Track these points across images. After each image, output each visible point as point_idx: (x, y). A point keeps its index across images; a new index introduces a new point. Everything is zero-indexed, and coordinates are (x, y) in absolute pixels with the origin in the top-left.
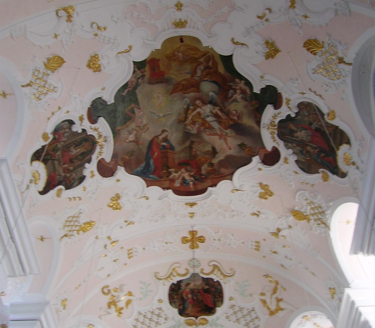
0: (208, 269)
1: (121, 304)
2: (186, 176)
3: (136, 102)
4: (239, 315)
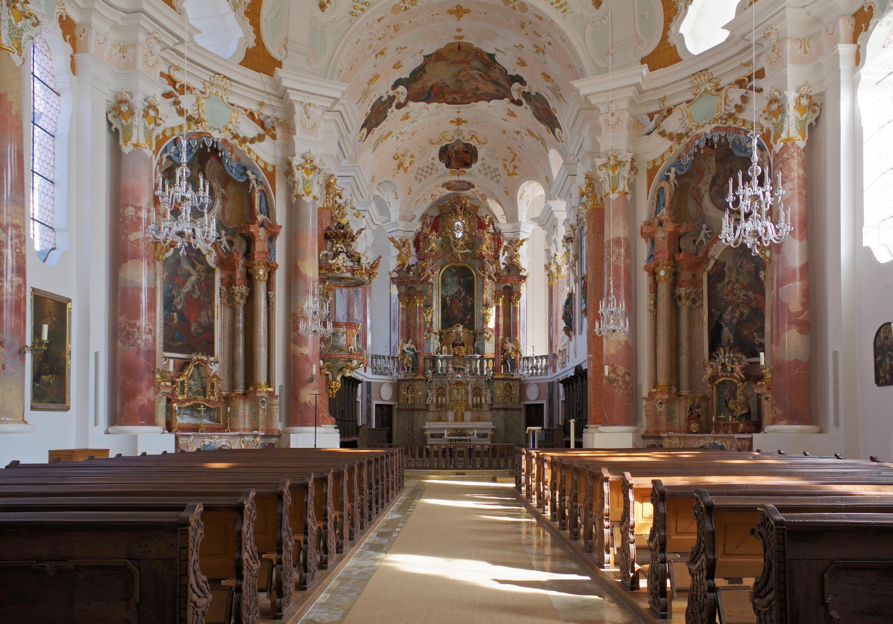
0: (467, 137)
1: (407, 164)
2: (457, 97)
3: (424, 72)
4: (488, 171)
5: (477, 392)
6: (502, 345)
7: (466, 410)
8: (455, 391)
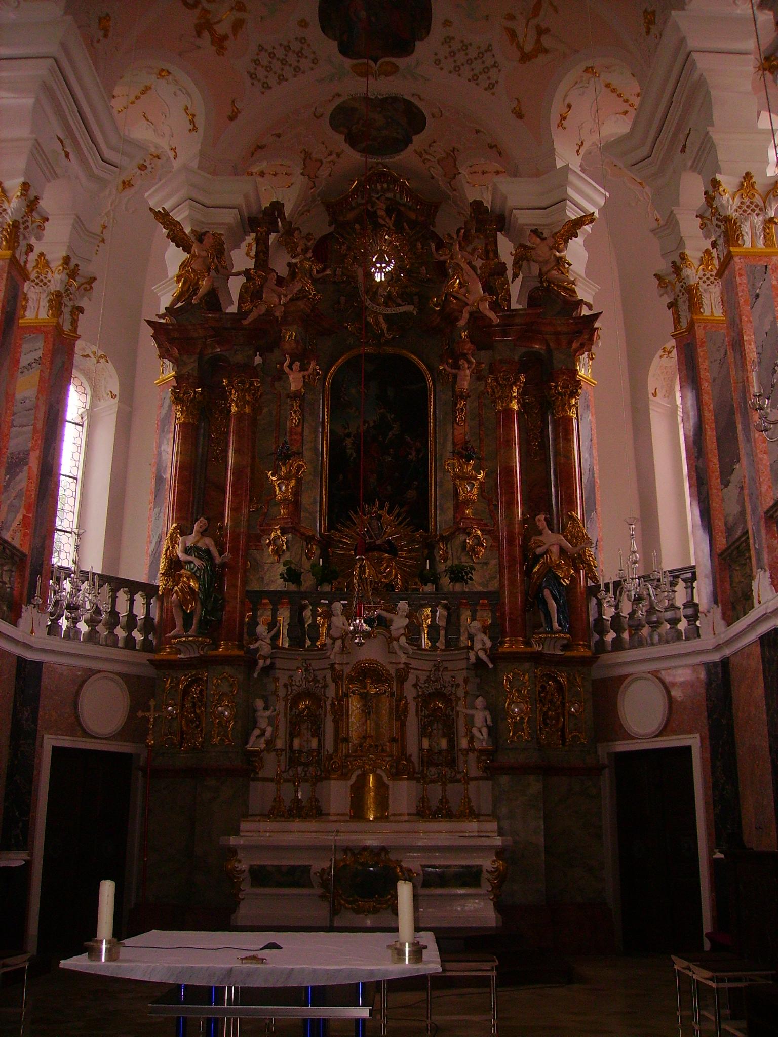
1: (223, 29)
5: (438, 710)
6: (526, 538)
7: (396, 775)
8: (355, 705)
